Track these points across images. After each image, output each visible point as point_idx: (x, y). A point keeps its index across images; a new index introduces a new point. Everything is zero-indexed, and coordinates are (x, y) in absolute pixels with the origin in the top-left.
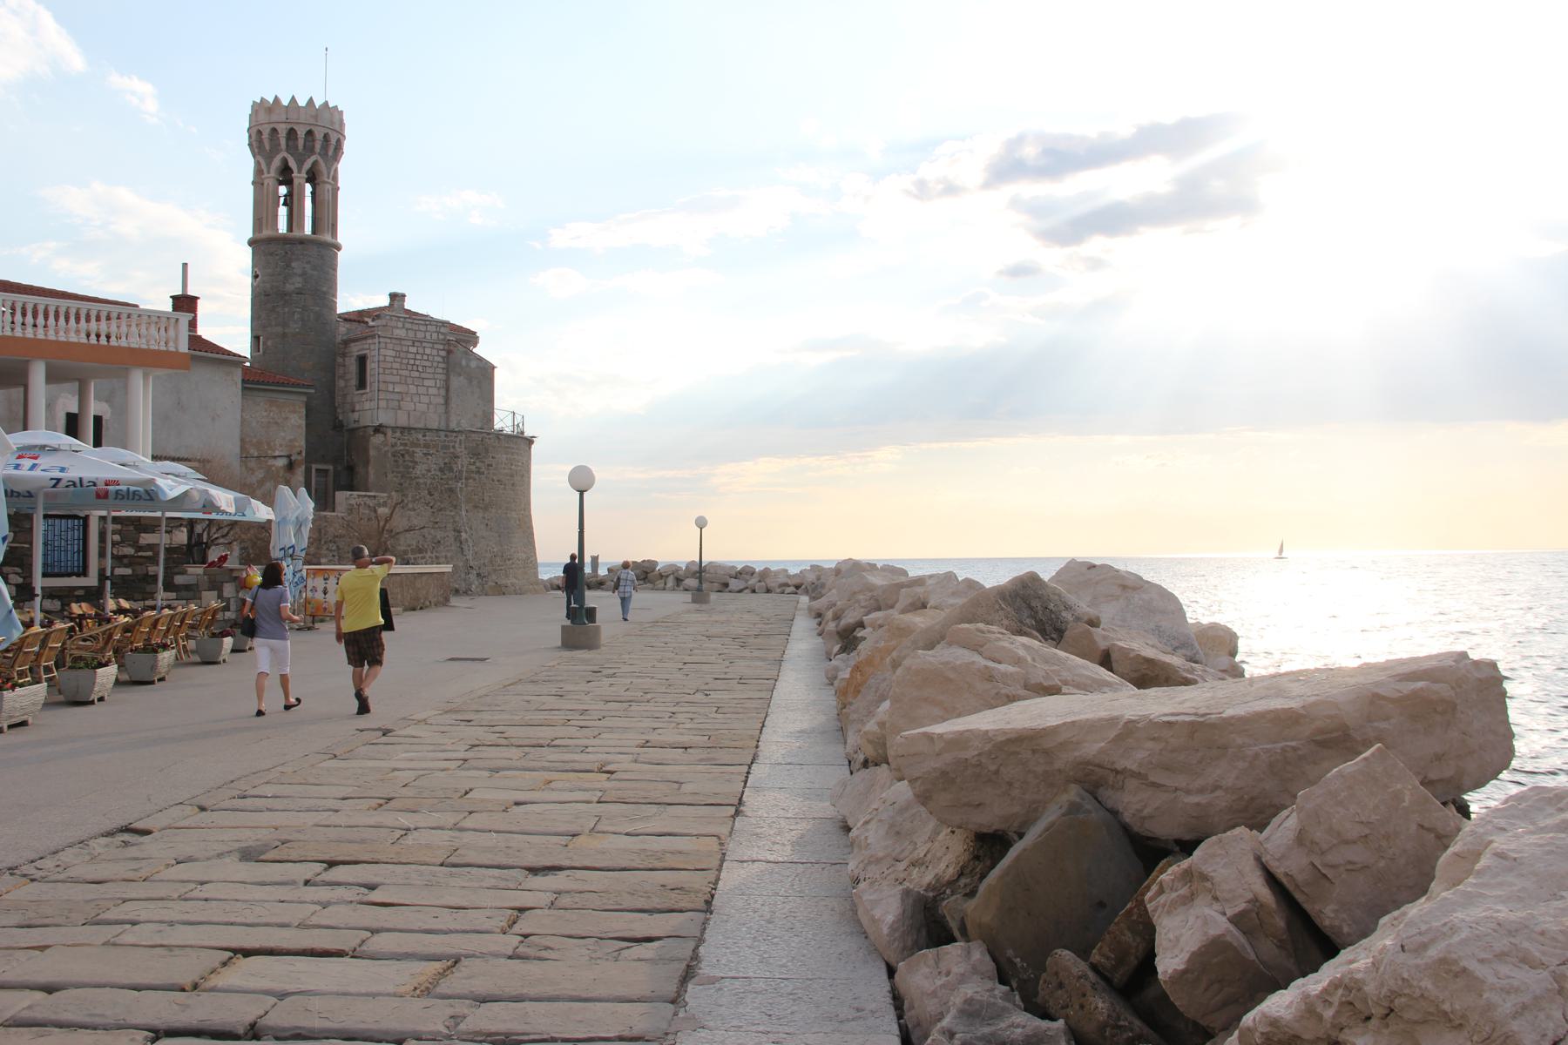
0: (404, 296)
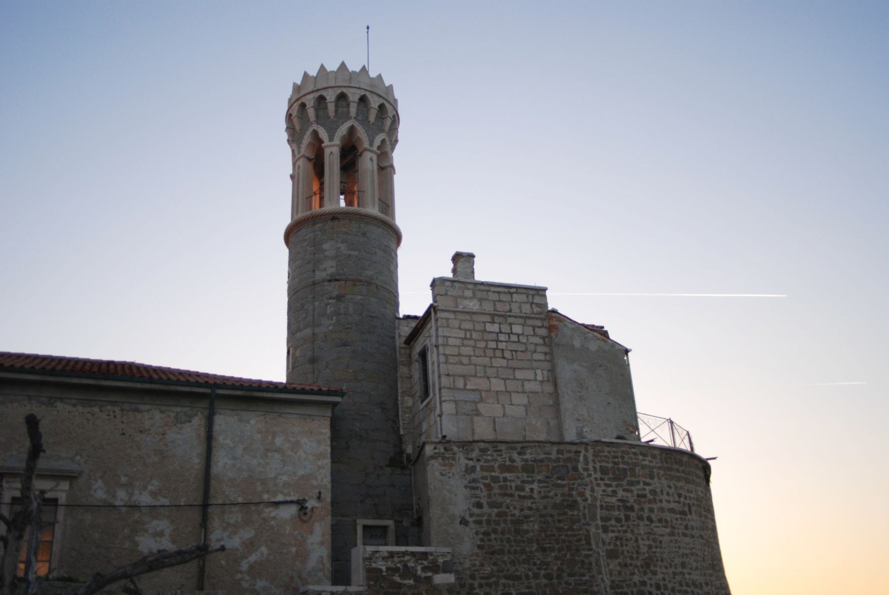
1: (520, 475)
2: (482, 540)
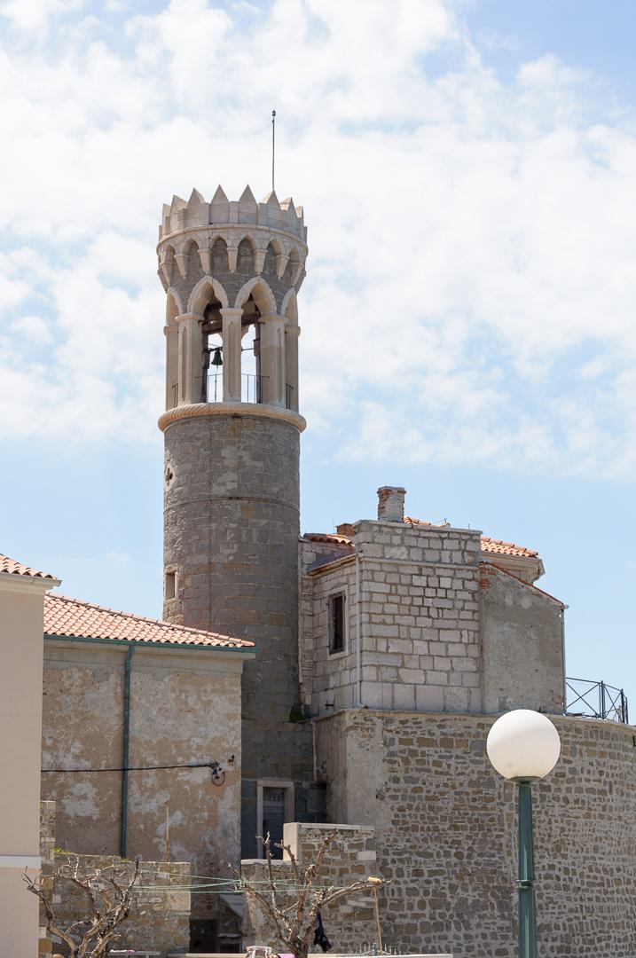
0: (402, 492)
2: (396, 816)
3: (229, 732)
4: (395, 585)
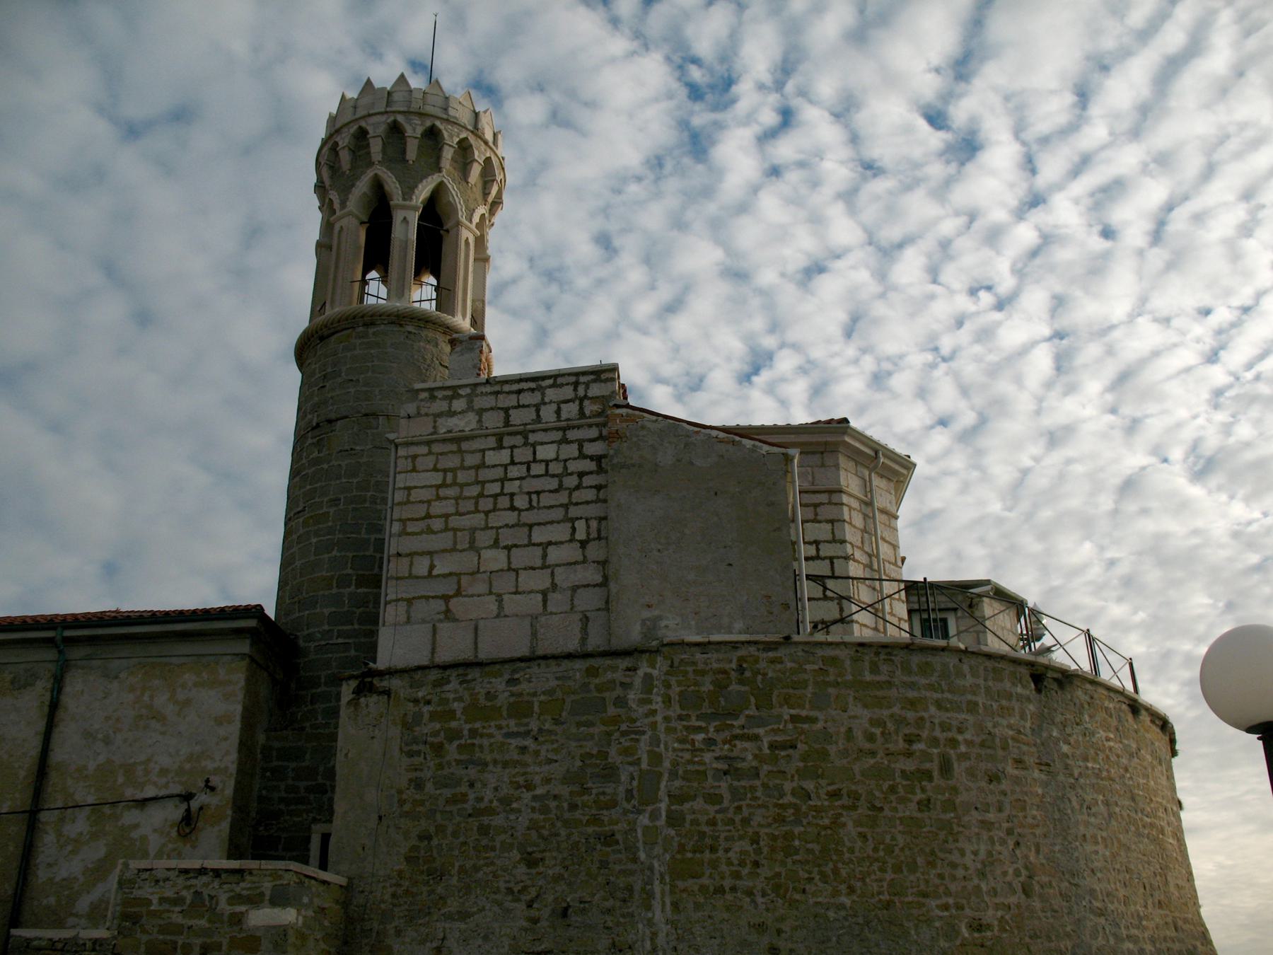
1: (504, 723)
3: (217, 744)
4: (454, 470)
